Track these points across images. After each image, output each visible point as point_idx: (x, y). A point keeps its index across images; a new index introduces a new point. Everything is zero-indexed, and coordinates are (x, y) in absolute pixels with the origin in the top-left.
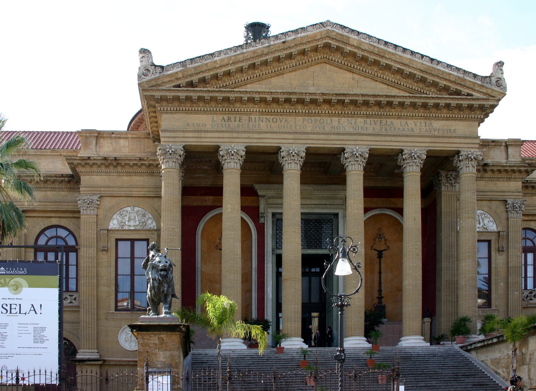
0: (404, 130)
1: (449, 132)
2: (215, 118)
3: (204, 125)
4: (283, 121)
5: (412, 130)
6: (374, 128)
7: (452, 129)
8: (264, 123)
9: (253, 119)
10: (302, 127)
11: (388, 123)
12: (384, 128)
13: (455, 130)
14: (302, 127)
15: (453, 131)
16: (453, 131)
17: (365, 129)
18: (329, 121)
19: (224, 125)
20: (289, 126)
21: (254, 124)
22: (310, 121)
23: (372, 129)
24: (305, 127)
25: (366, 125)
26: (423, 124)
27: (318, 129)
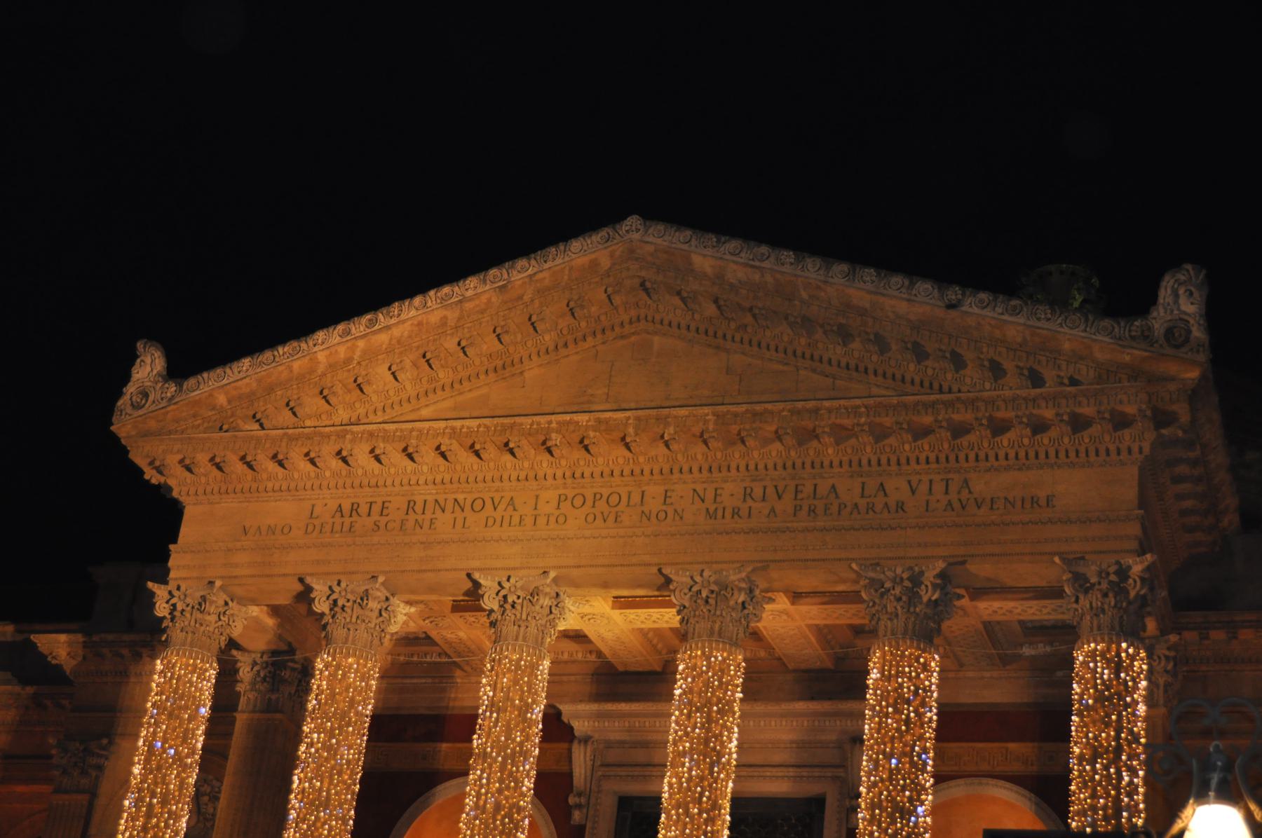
0: (871, 508)
1: (1028, 505)
2: (317, 511)
3: (286, 530)
4: (501, 507)
5: (900, 506)
6: (773, 510)
7: (1042, 494)
8: (448, 516)
9: (419, 508)
10: (552, 519)
11: (823, 489)
12: (806, 508)
13: (1049, 499)
14: (552, 519)
15: (1043, 502)
16: (1043, 502)
17: (744, 513)
18: (636, 498)
19: (337, 527)
20: (516, 520)
21: (420, 518)
22: (578, 501)
23: (766, 512)
24: (561, 519)
25: (750, 502)
26: (939, 488)
27: (599, 521)
